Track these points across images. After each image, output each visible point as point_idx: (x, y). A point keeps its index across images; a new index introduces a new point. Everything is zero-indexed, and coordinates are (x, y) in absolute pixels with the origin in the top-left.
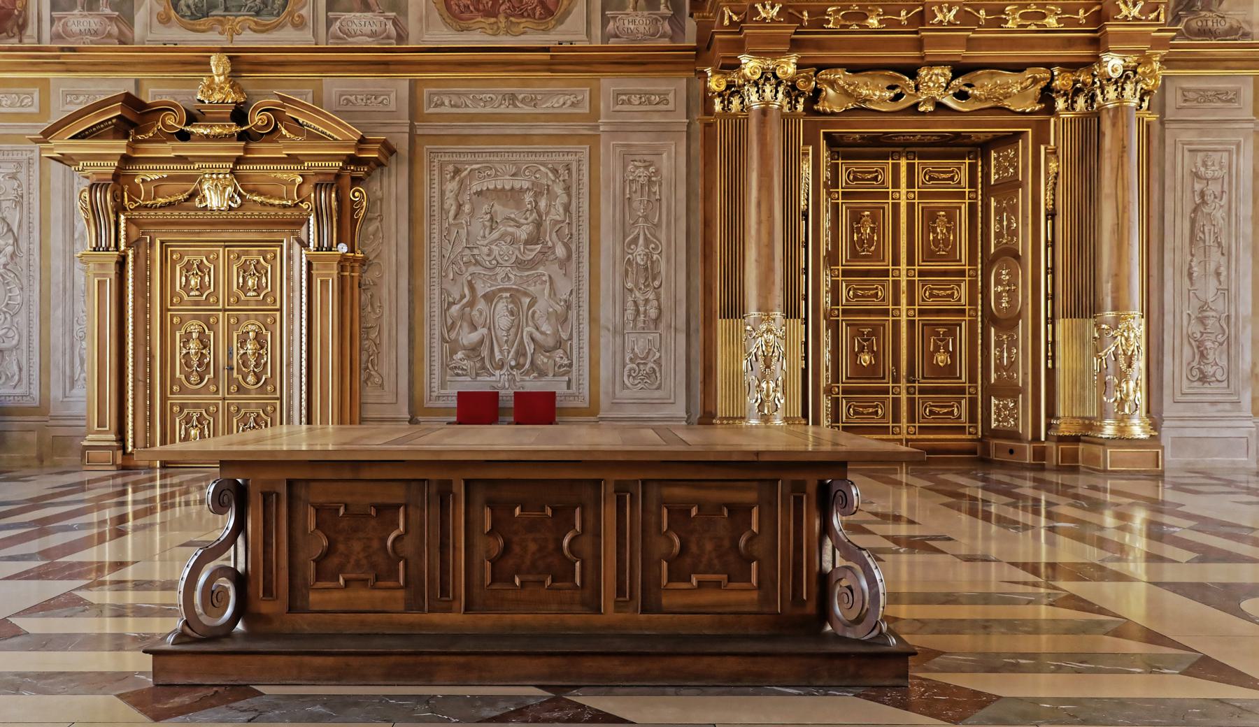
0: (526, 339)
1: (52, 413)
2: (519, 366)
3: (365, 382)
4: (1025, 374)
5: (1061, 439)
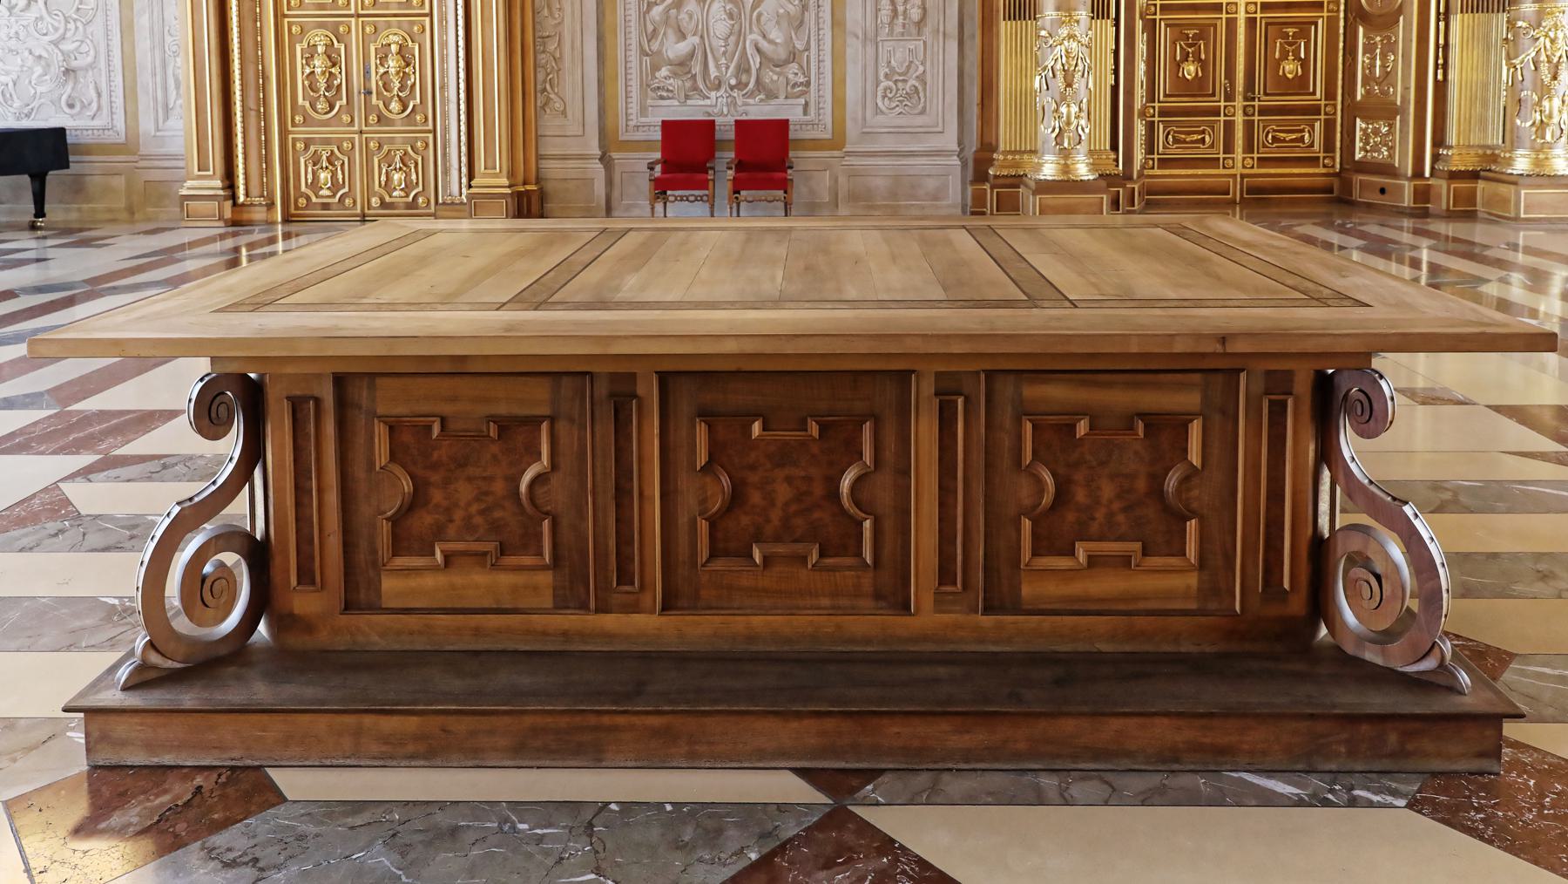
0: (750, 50)
1: (143, 151)
2: (740, 85)
3: (543, 108)
4: (1406, 89)
5: (1454, 176)
